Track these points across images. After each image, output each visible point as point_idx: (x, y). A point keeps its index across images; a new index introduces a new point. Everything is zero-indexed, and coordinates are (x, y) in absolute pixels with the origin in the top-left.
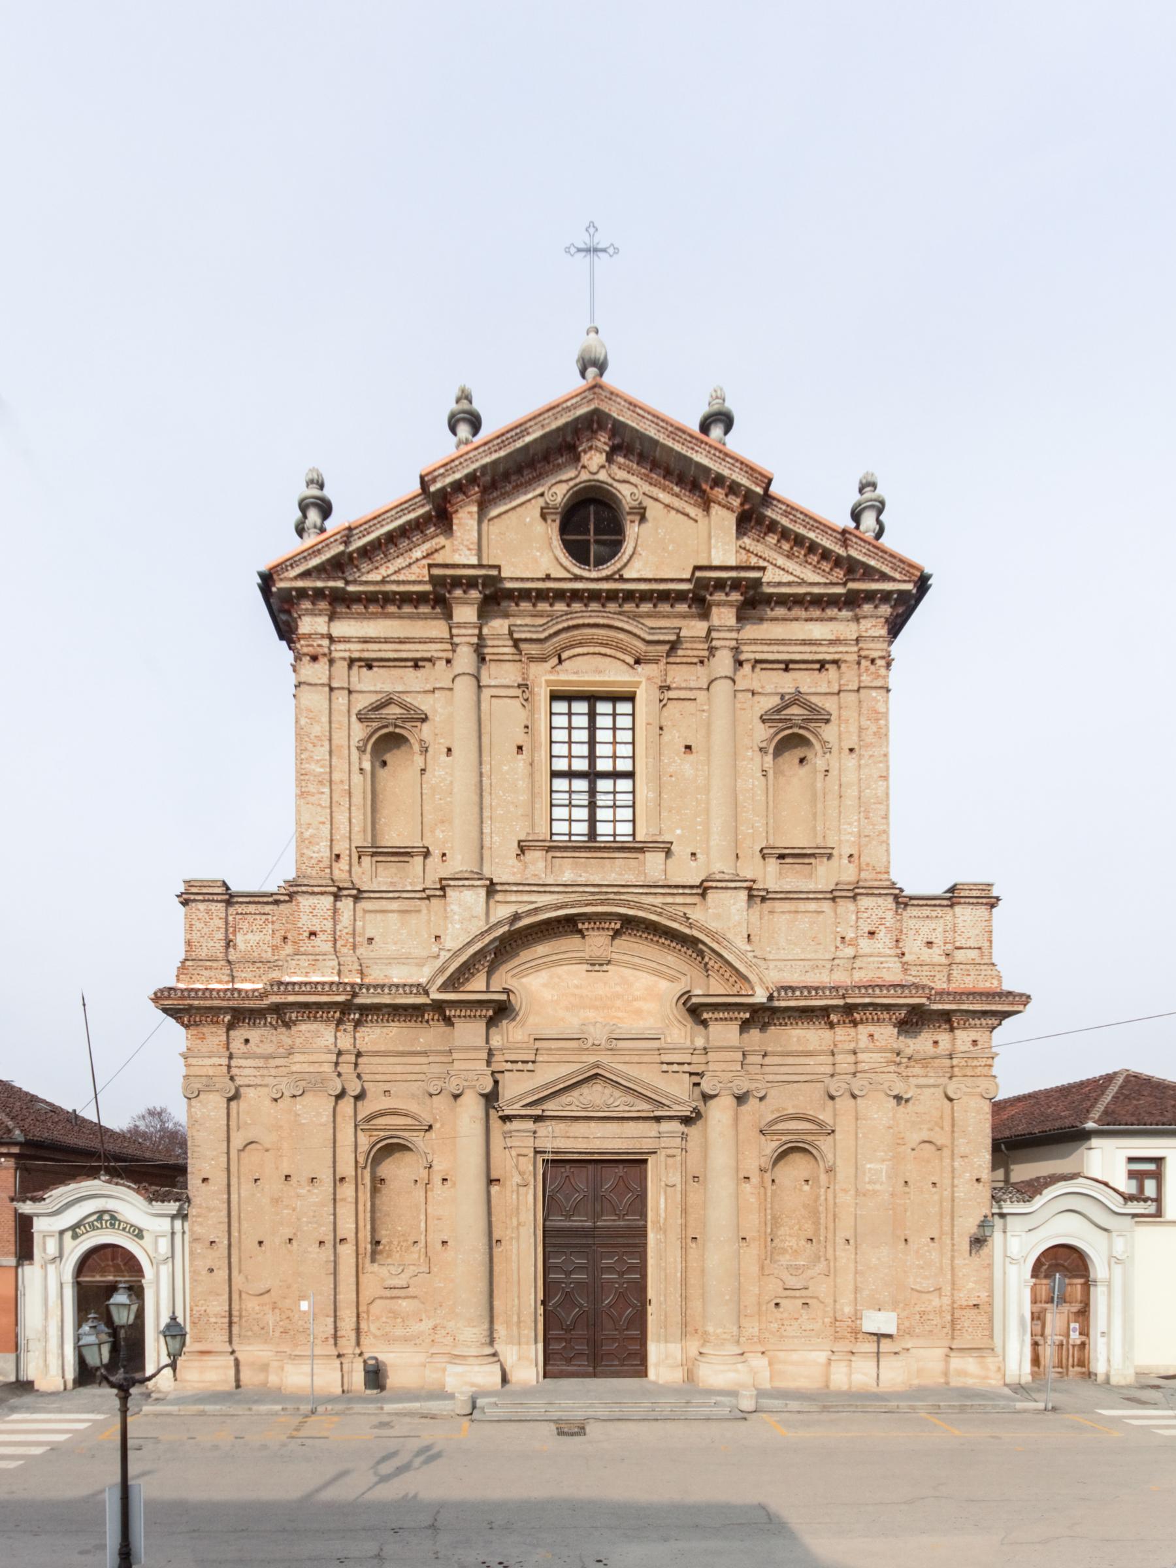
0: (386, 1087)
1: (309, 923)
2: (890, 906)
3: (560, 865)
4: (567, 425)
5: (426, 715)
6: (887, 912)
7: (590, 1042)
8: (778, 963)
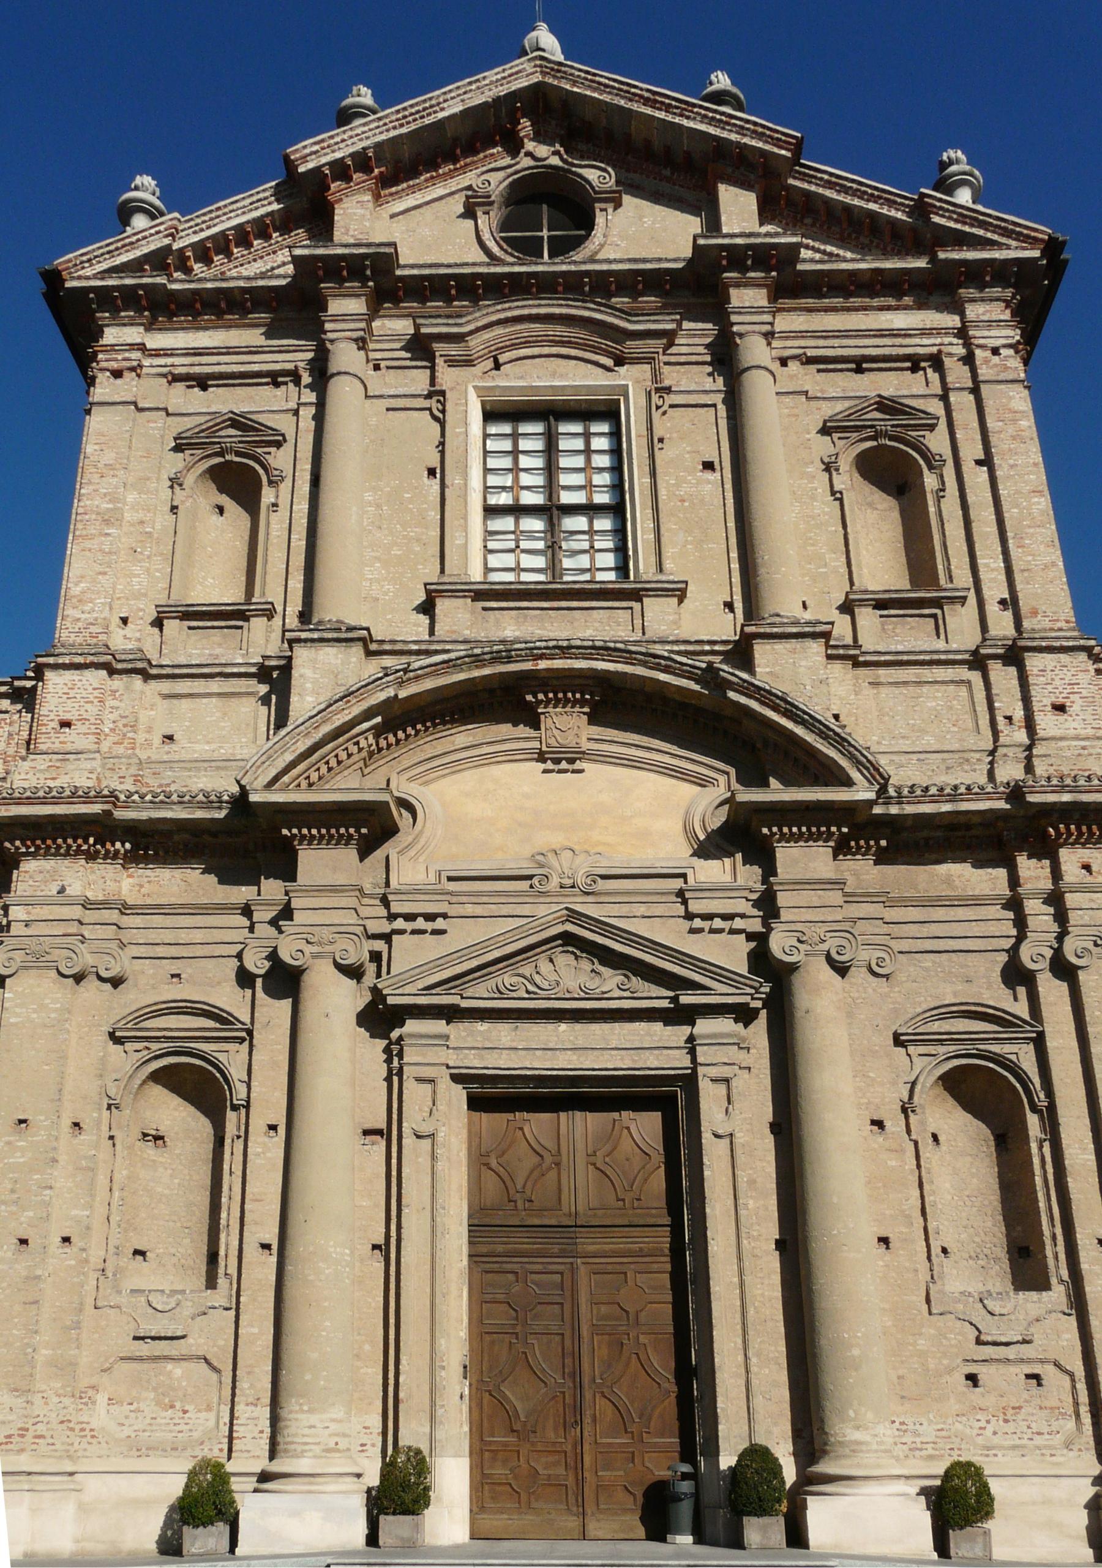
0: (174, 967)
1: (60, 709)
2: (1083, 666)
3: (497, 621)
4: (497, 100)
5: (283, 435)
6: (1081, 675)
7: (555, 881)
8: (895, 757)
